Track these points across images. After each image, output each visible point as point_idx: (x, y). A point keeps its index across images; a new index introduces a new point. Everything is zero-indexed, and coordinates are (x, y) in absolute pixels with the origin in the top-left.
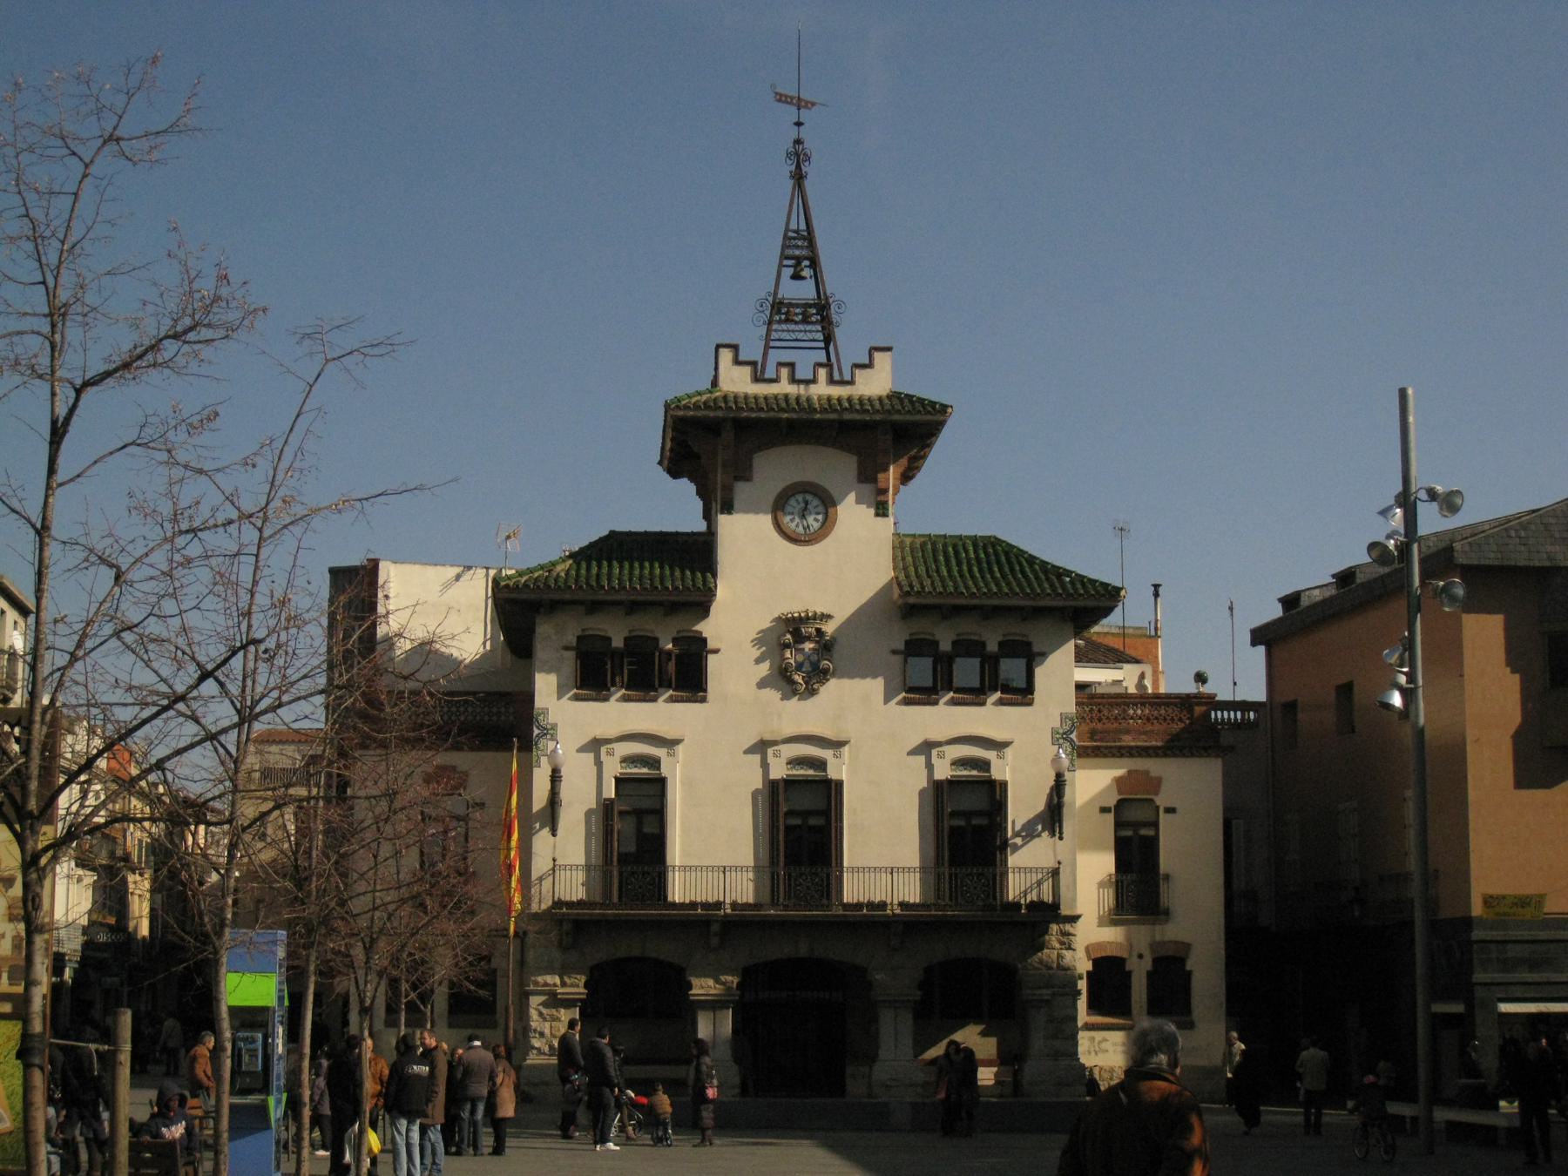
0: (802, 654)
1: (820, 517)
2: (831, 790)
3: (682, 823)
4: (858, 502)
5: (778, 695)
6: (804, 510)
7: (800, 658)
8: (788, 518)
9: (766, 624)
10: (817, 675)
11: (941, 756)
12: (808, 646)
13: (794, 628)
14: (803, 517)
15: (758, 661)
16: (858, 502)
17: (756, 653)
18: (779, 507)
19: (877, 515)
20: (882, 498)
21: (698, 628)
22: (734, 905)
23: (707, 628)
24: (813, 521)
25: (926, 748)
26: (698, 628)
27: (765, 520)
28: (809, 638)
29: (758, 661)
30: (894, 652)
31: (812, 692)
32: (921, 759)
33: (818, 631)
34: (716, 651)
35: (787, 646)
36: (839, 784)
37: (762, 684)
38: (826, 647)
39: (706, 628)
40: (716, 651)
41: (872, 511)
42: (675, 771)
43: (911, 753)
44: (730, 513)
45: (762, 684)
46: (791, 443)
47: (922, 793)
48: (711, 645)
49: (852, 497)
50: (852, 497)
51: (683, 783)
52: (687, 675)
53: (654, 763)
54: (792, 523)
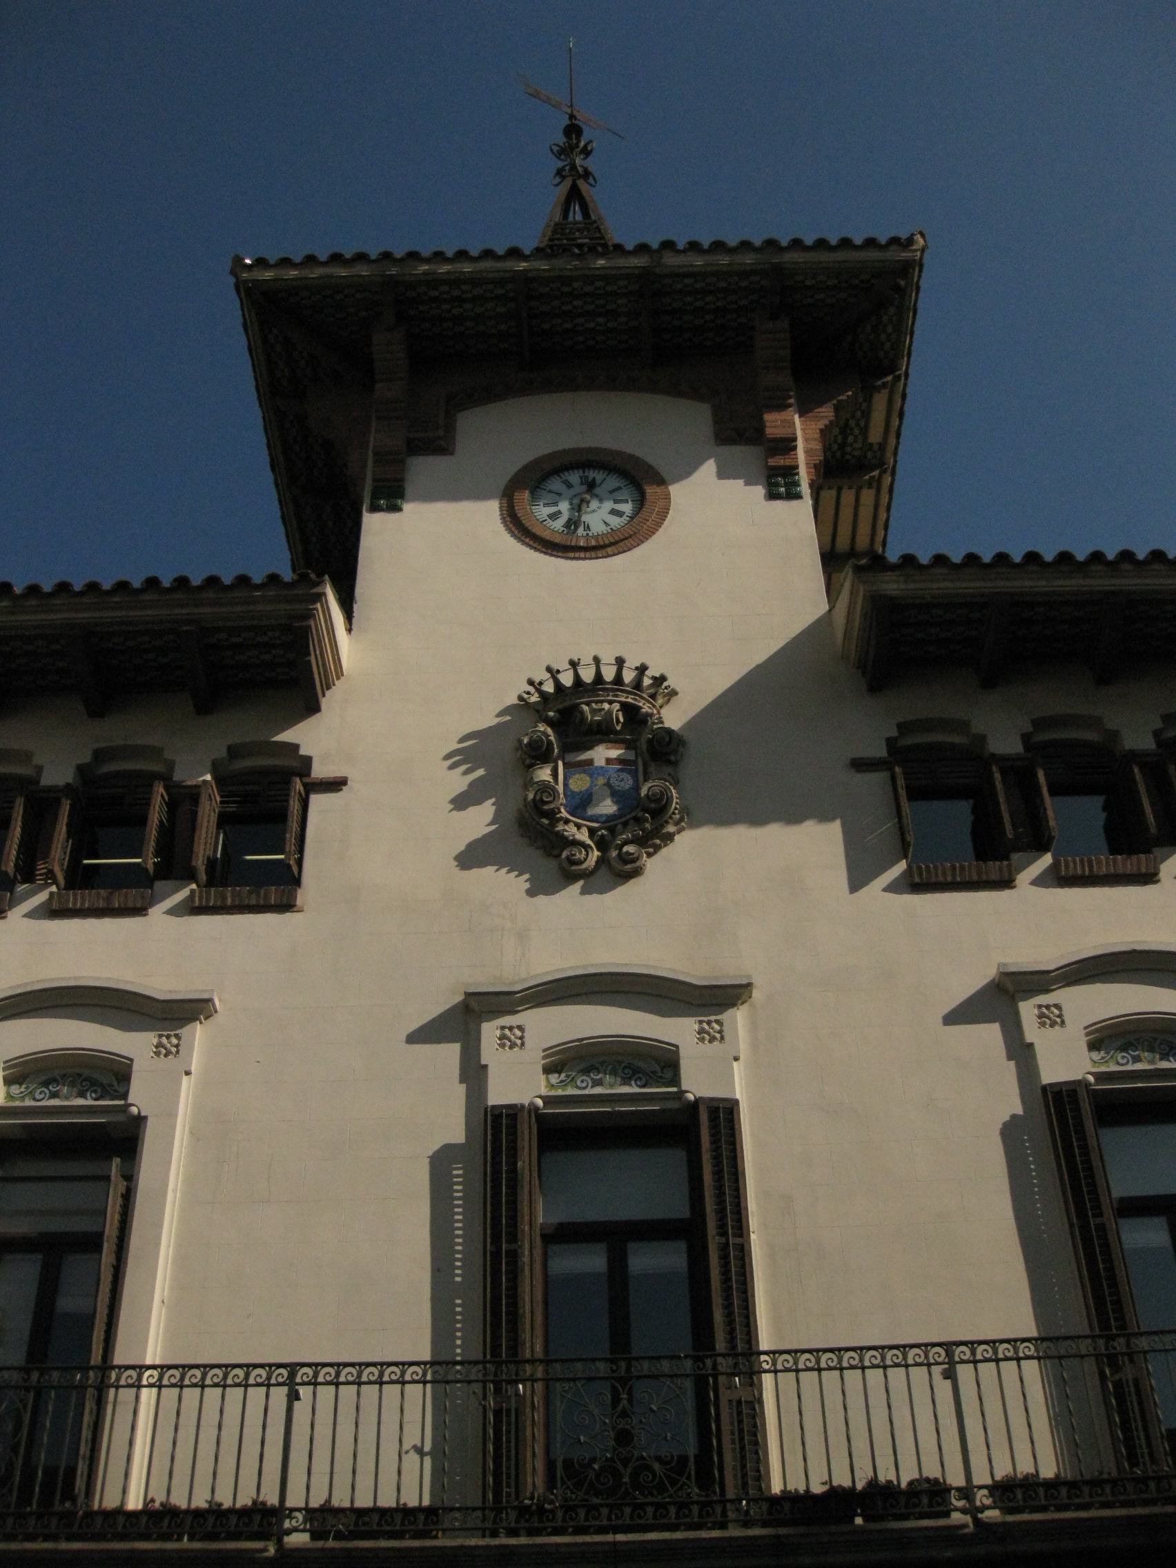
0: (585, 776)
1: (627, 508)
2: (702, 1138)
3: (182, 1262)
4: (722, 475)
5: (521, 883)
6: (587, 496)
7: (580, 783)
8: (543, 511)
9: (486, 719)
10: (640, 828)
11: (1052, 1018)
12: (603, 754)
13: (565, 715)
14: (578, 508)
15: (461, 802)
16: (722, 475)
17: (459, 782)
18: (520, 488)
19: (772, 496)
20: (779, 461)
21: (287, 736)
22: (322, 1518)
23: (316, 739)
24: (601, 517)
25: (1002, 998)
26: (287, 736)
27: (485, 515)
28: (602, 732)
29: (461, 802)
30: (860, 765)
31: (623, 871)
32: (991, 1034)
33: (630, 710)
34: (336, 785)
35: (538, 754)
36: (724, 1115)
37: (471, 857)
38: (659, 750)
39: (316, 739)
40: (336, 785)
41: (759, 491)
42: (177, 1098)
43: (955, 1017)
44: (397, 509)
45: (471, 857)
46: (548, 387)
47: (1011, 1132)
48: (319, 771)
49: (709, 467)
50: (709, 467)
51: (195, 1135)
52: (249, 845)
53: (111, 1075)
54: (549, 514)
